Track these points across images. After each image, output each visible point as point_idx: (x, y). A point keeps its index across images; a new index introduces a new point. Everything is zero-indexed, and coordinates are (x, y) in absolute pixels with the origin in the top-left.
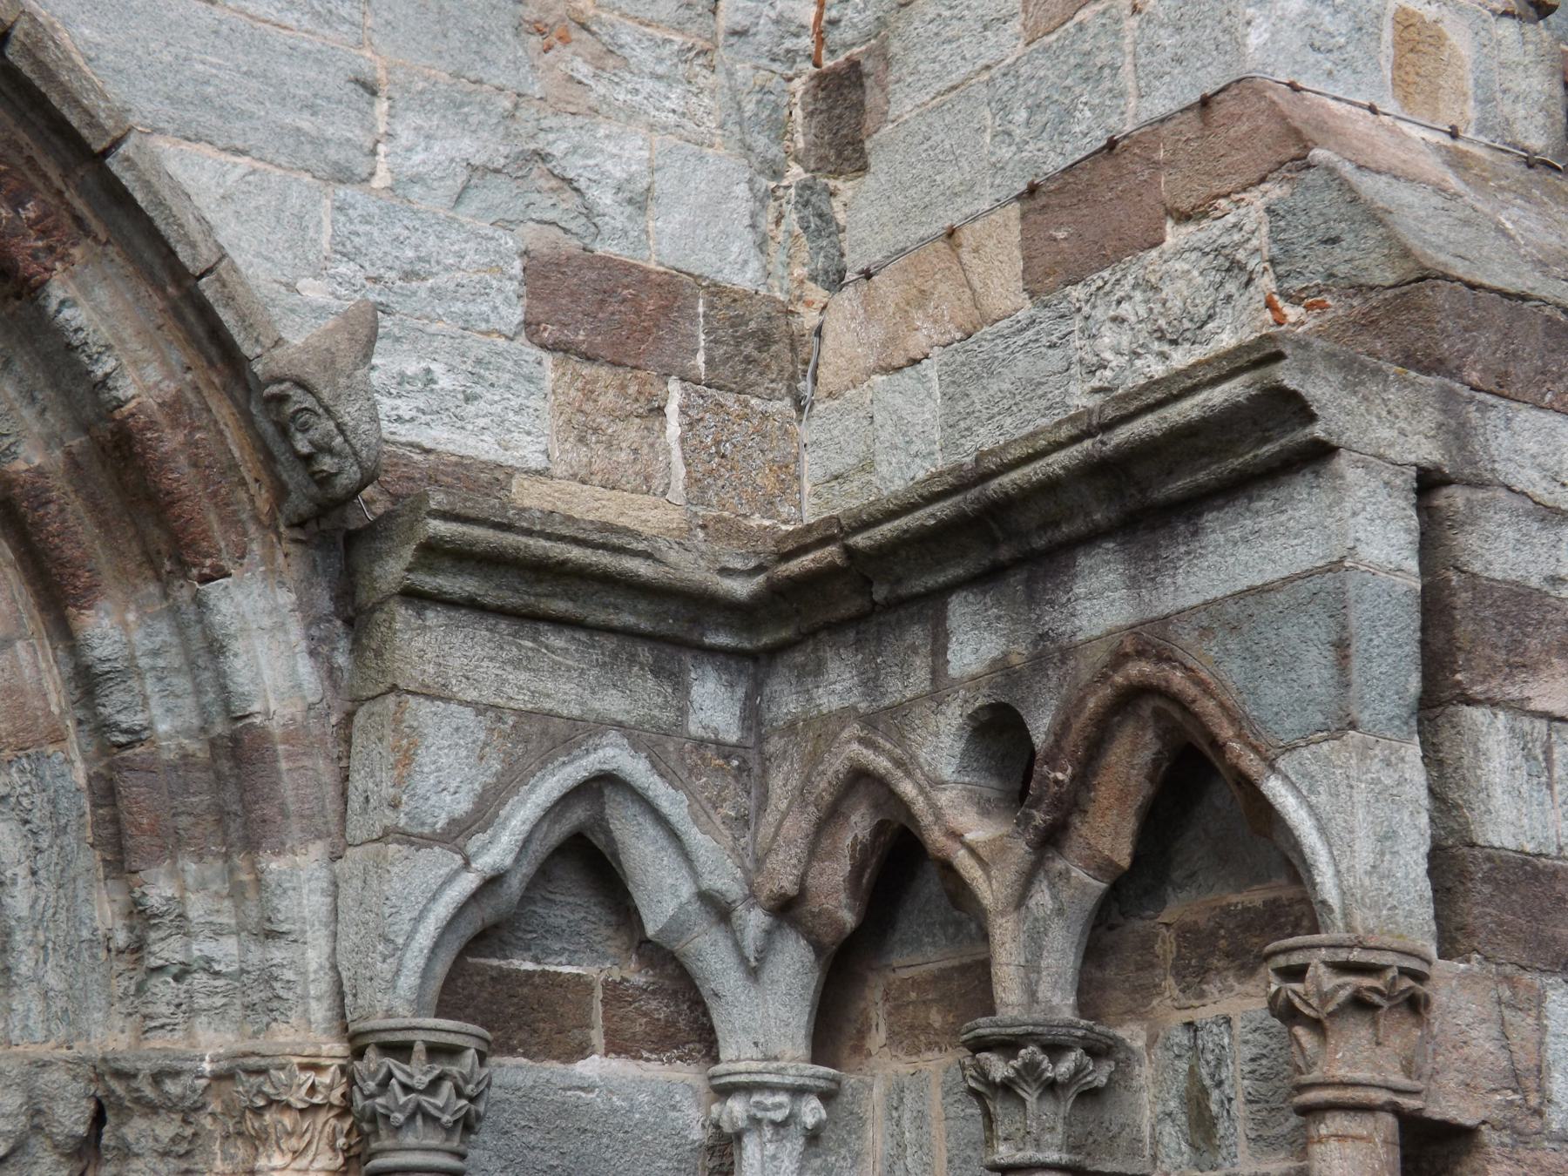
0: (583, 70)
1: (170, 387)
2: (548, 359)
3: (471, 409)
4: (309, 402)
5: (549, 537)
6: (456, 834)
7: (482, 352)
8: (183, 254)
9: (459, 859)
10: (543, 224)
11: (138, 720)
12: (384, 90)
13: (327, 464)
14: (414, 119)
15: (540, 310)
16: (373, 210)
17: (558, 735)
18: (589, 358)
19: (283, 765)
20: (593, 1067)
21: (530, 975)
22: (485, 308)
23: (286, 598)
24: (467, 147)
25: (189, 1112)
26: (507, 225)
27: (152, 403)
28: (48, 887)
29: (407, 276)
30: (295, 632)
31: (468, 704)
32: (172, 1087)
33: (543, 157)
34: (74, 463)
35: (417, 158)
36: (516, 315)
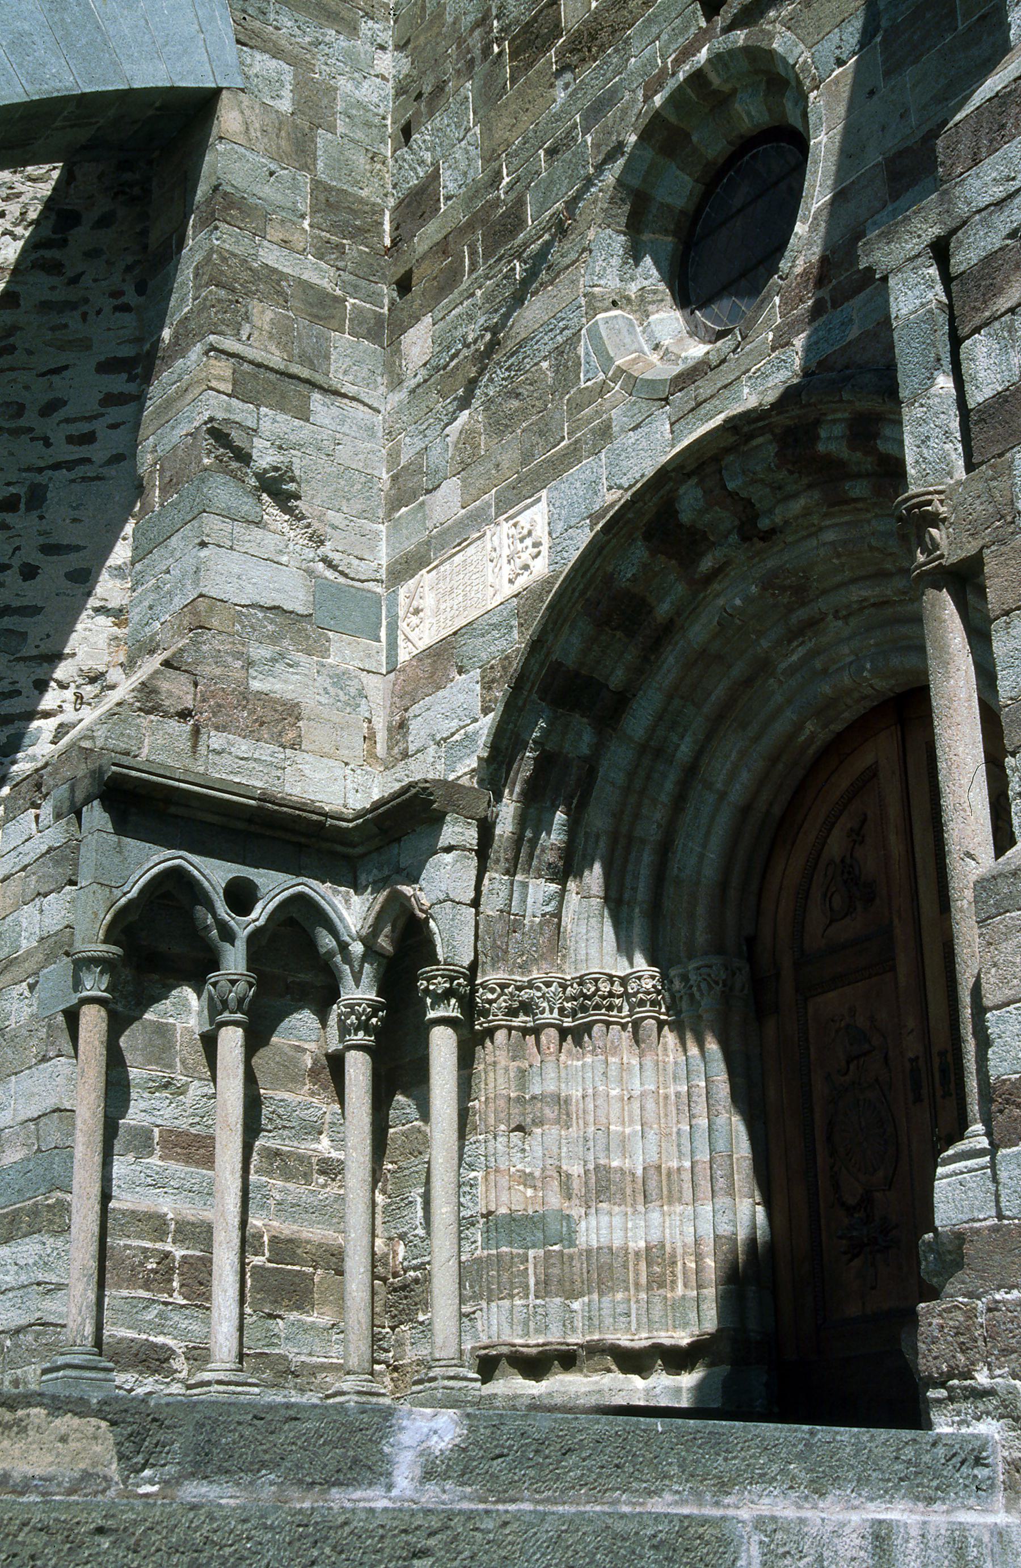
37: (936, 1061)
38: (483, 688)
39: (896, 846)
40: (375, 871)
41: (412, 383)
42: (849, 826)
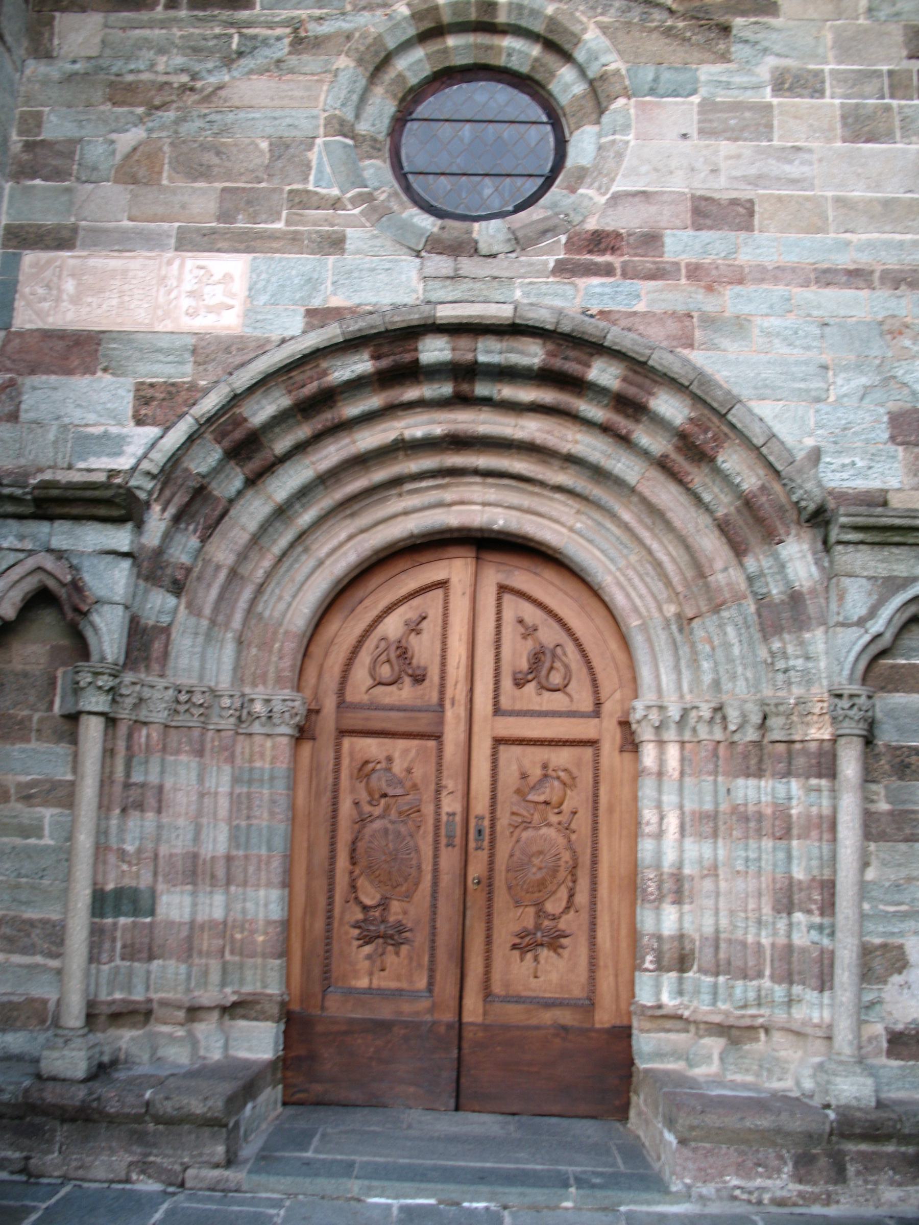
0: (907, 343)
1: (759, 483)
2: (900, 448)
6: (861, 622)
8: (755, 441)
11: (764, 591)
13: (803, 504)
14: (843, 375)
21: (904, 665)
23: (805, 547)
24: (864, 380)
25: (789, 715)
29: (845, 429)
30: (810, 558)
32: (781, 708)
33: (894, 377)
34: (738, 511)
36: (886, 436)
40: (11, 538)
41: (69, 67)
42: (408, 616)
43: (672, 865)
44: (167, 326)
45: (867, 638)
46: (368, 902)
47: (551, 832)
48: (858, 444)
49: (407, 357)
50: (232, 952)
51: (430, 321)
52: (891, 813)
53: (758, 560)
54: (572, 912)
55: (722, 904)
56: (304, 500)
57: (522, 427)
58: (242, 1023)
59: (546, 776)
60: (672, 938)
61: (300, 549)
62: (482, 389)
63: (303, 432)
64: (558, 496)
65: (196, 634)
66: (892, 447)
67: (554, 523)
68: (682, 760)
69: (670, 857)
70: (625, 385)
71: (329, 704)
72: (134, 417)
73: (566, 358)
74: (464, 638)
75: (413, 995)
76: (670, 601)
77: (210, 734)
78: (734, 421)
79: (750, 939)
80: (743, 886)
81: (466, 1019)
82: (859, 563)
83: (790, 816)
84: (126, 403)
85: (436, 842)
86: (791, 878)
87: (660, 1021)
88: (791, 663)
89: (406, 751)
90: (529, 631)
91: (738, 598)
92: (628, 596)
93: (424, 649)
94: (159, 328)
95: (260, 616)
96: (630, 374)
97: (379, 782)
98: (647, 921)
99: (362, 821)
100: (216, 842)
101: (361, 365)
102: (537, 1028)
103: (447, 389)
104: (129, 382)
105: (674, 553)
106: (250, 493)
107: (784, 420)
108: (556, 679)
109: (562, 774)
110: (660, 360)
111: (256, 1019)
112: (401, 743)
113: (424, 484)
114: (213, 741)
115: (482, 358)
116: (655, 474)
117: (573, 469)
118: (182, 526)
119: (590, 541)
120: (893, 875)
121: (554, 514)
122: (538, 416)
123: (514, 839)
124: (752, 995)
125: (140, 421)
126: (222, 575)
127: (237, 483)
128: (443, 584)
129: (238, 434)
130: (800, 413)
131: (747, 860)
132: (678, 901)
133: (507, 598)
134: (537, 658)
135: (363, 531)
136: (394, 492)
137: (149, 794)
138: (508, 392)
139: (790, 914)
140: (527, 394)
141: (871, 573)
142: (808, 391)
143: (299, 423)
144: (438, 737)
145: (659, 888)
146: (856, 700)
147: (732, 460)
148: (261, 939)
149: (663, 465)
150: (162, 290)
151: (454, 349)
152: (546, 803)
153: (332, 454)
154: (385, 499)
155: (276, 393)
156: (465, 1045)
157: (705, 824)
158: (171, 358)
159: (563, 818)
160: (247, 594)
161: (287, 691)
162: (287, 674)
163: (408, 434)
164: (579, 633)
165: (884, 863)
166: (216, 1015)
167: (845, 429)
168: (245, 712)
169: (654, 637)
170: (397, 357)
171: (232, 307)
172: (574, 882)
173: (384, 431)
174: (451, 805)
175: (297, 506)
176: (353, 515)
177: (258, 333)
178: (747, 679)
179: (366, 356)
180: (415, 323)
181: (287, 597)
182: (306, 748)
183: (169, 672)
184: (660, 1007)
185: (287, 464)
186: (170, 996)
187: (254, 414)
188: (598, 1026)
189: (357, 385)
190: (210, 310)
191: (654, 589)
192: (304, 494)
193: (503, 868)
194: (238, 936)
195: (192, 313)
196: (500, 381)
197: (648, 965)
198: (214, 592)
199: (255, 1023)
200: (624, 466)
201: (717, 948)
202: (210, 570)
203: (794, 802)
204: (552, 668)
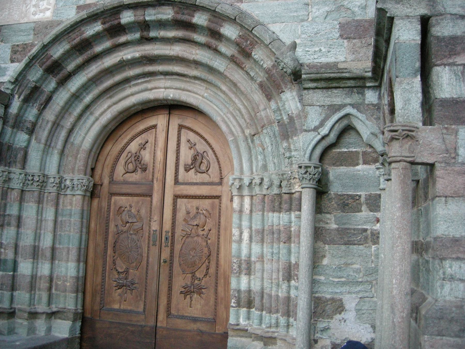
1: (272, 64)
2: (345, 41)
3: (329, 54)
4: (279, 61)
5: (327, 73)
6: (316, 129)
7: (331, 43)
8: (266, 42)
9: (317, 133)
10: (344, 17)
12: (310, 4)
14: (316, 7)
15: (343, 32)
16: (308, 24)
17: (334, 109)
18: (354, 39)
19: (296, 121)
20: (359, 167)
21: (346, 152)
22: (332, 35)
23: (294, 93)
24: (327, 8)
26: (336, 20)
27: (270, 67)
28: (274, 146)
29: (316, 34)
30: (297, 99)
31: (317, 106)
32: (285, 176)
33: (343, 6)
35: (316, 14)
36: (338, 35)
37: (164, 234)
38: (12, 51)
39: (160, 155)
42: (140, 142)
43: (245, 256)
44: (26, 20)
45: (319, 137)
46: (120, 270)
47: (200, 240)
48: (323, 40)
49: (116, 22)
50: (56, 290)
51: (122, 4)
52: (337, 230)
53: (277, 103)
54: (208, 277)
55: (265, 276)
56: (87, 91)
57: (173, 50)
58: (59, 321)
59: (197, 213)
60: (245, 291)
61: (88, 113)
62: (152, 34)
63: (79, 60)
64: (196, 82)
65: (39, 151)
66: (341, 41)
67: (195, 95)
68: (252, 205)
69: (245, 252)
70: (209, 23)
71: (106, 181)
72: (10, 59)
73: (183, 14)
74: (163, 150)
75: (138, 313)
76: (247, 128)
77: (46, 194)
78: (255, 33)
79: (273, 293)
80: (270, 266)
81: (159, 324)
82: (315, 99)
83: (291, 231)
84: (8, 53)
85: (149, 243)
86: (290, 263)
87: (238, 332)
88: (293, 153)
89: (138, 202)
90: (192, 146)
91: (271, 123)
92: (228, 126)
93: (146, 156)
94: (22, 21)
95: (73, 144)
96: (212, 18)
97: (125, 217)
98: (233, 283)
99: (118, 233)
100: (46, 242)
101: (98, 27)
102: (190, 331)
103: (137, 35)
104: (9, 45)
105: (246, 104)
106: (61, 89)
107: (284, 32)
108: (203, 168)
109: (204, 212)
110: (224, 8)
111: (65, 320)
112: (136, 199)
113: (140, 81)
114: (47, 197)
115: (147, 18)
116: (232, 65)
117: (200, 69)
118: (31, 104)
119: (211, 101)
120: (337, 262)
121: (195, 90)
122: (180, 44)
123: (183, 242)
124: (273, 321)
125: (12, 61)
126: (50, 125)
127: (53, 85)
128: (155, 127)
129: (49, 63)
130: (293, 28)
131: (272, 253)
132: (249, 272)
133: (183, 131)
134: (195, 159)
135: (115, 103)
136: (127, 85)
137: (13, 219)
138: (163, 33)
139: (289, 281)
140: (171, 34)
141: (322, 103)
142: (298, 17)
143: (78, 57)
144: (151, 196)
145: (240, 267)
146: (309, 170)
147: (258, 54)
148: (68, 284)
149: (232, 59)
150: (24, 5)
151: (135, 16)
152: (197, 225)
153: (93, 69)
154: (124, 89)
155: (64, 43)
156: (157, 336)
157: (261, 235)
158: (26, 33)
159: (205, 233)
160: (63, 134)
161: (81, 175)
162: (82, 168)
163: (125, 58)
164: (214, 146)
165: (333, 256)
166: (44, 316)
167: (316, 34)
168: (63, 185)
169: (240, 145)
170: (112, 22)
171: (49, 9)
172: (209, 263)
173: (116, 57)
174: (155, 226)
175: (85, 94)
176: (111, 97)
177: (58, 19)
178: (274, 163)
179: (99, 23)
180: (116, 5)
181: (83, 135)
182: (95, 202)
183: (27, 167)
184: (238, 325)
185: (76, 76)
186: (23, 307)
187: (55, 54)
188: (217, 332)
189: (97, 37)
190: (41, 11)
191: (240, 122)
192: (85, 87)
193: (178, 256)
194: (59, 283)
195: (35, 14)
196: (160, 29)
197: (232, 304)
198: (46, 133)
199: (64, 321)
200: (219, 64)
201: (262, 297)
202: (45, 123)
203: (293, 224)
204: (202, 162)
